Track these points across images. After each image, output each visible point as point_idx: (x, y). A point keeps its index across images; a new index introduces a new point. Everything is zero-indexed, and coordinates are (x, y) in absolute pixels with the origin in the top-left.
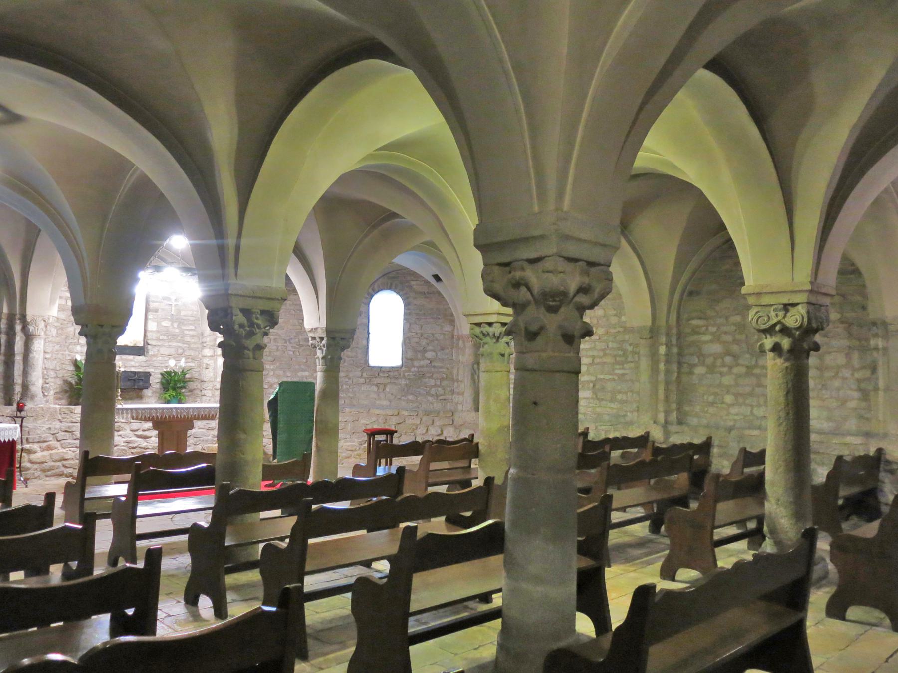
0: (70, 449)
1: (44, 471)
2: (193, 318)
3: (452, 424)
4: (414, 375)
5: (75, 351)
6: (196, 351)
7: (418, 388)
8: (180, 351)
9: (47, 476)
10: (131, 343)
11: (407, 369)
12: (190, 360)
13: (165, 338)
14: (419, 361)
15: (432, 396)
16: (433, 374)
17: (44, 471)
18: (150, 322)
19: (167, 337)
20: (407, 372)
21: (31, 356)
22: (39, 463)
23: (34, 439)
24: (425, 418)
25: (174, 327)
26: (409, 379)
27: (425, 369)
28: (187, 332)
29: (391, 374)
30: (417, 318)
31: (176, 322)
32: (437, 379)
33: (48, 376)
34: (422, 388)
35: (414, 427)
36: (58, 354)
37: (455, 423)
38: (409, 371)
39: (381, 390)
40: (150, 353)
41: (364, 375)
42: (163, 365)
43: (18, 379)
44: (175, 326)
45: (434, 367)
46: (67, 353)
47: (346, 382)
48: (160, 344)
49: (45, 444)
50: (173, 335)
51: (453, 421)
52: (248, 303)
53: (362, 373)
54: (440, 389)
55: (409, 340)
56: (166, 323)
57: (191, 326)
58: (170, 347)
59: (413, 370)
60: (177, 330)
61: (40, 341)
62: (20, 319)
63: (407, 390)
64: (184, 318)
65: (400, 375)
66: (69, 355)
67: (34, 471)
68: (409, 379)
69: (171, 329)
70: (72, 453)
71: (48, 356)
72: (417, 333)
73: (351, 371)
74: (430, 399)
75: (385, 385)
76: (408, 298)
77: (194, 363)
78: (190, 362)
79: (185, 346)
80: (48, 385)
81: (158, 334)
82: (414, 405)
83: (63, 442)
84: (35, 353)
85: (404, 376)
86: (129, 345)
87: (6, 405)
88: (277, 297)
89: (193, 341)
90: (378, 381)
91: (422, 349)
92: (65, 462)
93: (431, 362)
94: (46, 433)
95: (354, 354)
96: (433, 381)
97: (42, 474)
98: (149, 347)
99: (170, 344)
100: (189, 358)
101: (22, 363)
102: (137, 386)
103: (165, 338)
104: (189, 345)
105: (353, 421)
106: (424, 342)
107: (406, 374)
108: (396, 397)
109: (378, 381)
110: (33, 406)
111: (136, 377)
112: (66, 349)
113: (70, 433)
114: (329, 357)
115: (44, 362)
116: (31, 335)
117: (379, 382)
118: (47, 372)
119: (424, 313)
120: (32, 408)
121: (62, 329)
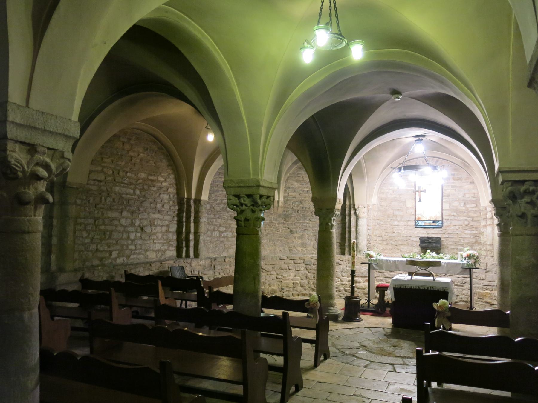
2: (475, 199)
5: (394, 225)
6: (478, 222)
8: (466, 223)
12: (474, 229)
13: (455, 214)
21: (358, 228)
22: (362, 289)
28: (470, 209)
31: (462, 202)
33: (370, 239)
36: (383, 226)
40: (445, 225)
42: (455, 233)
46: (389, 226)
48: (452, 218)
52: (237, 191)
56: (456, 204)
57: (473, 204)
58: (459, 220)
60: (464, 208)
61: (363, 219)
64: (469, 199)
66: (390, 227)
71: (369, 228)
78: (474, 230)
79: (469, 219)
80: (370, 245)
83: (377, 278)
84: (360, 226)
88: (253, 185)
89: (475, 215)
99: (459, 218)
100: (473, 228)
101: (355, 232)
102: (431, 246)
103: (455, 214)
104: (472, 218)
110: (360, 256)
111: (430, 240)
113: (382, 274)
114: (502, 224)
115: (367, 231)
120: (359, 257)
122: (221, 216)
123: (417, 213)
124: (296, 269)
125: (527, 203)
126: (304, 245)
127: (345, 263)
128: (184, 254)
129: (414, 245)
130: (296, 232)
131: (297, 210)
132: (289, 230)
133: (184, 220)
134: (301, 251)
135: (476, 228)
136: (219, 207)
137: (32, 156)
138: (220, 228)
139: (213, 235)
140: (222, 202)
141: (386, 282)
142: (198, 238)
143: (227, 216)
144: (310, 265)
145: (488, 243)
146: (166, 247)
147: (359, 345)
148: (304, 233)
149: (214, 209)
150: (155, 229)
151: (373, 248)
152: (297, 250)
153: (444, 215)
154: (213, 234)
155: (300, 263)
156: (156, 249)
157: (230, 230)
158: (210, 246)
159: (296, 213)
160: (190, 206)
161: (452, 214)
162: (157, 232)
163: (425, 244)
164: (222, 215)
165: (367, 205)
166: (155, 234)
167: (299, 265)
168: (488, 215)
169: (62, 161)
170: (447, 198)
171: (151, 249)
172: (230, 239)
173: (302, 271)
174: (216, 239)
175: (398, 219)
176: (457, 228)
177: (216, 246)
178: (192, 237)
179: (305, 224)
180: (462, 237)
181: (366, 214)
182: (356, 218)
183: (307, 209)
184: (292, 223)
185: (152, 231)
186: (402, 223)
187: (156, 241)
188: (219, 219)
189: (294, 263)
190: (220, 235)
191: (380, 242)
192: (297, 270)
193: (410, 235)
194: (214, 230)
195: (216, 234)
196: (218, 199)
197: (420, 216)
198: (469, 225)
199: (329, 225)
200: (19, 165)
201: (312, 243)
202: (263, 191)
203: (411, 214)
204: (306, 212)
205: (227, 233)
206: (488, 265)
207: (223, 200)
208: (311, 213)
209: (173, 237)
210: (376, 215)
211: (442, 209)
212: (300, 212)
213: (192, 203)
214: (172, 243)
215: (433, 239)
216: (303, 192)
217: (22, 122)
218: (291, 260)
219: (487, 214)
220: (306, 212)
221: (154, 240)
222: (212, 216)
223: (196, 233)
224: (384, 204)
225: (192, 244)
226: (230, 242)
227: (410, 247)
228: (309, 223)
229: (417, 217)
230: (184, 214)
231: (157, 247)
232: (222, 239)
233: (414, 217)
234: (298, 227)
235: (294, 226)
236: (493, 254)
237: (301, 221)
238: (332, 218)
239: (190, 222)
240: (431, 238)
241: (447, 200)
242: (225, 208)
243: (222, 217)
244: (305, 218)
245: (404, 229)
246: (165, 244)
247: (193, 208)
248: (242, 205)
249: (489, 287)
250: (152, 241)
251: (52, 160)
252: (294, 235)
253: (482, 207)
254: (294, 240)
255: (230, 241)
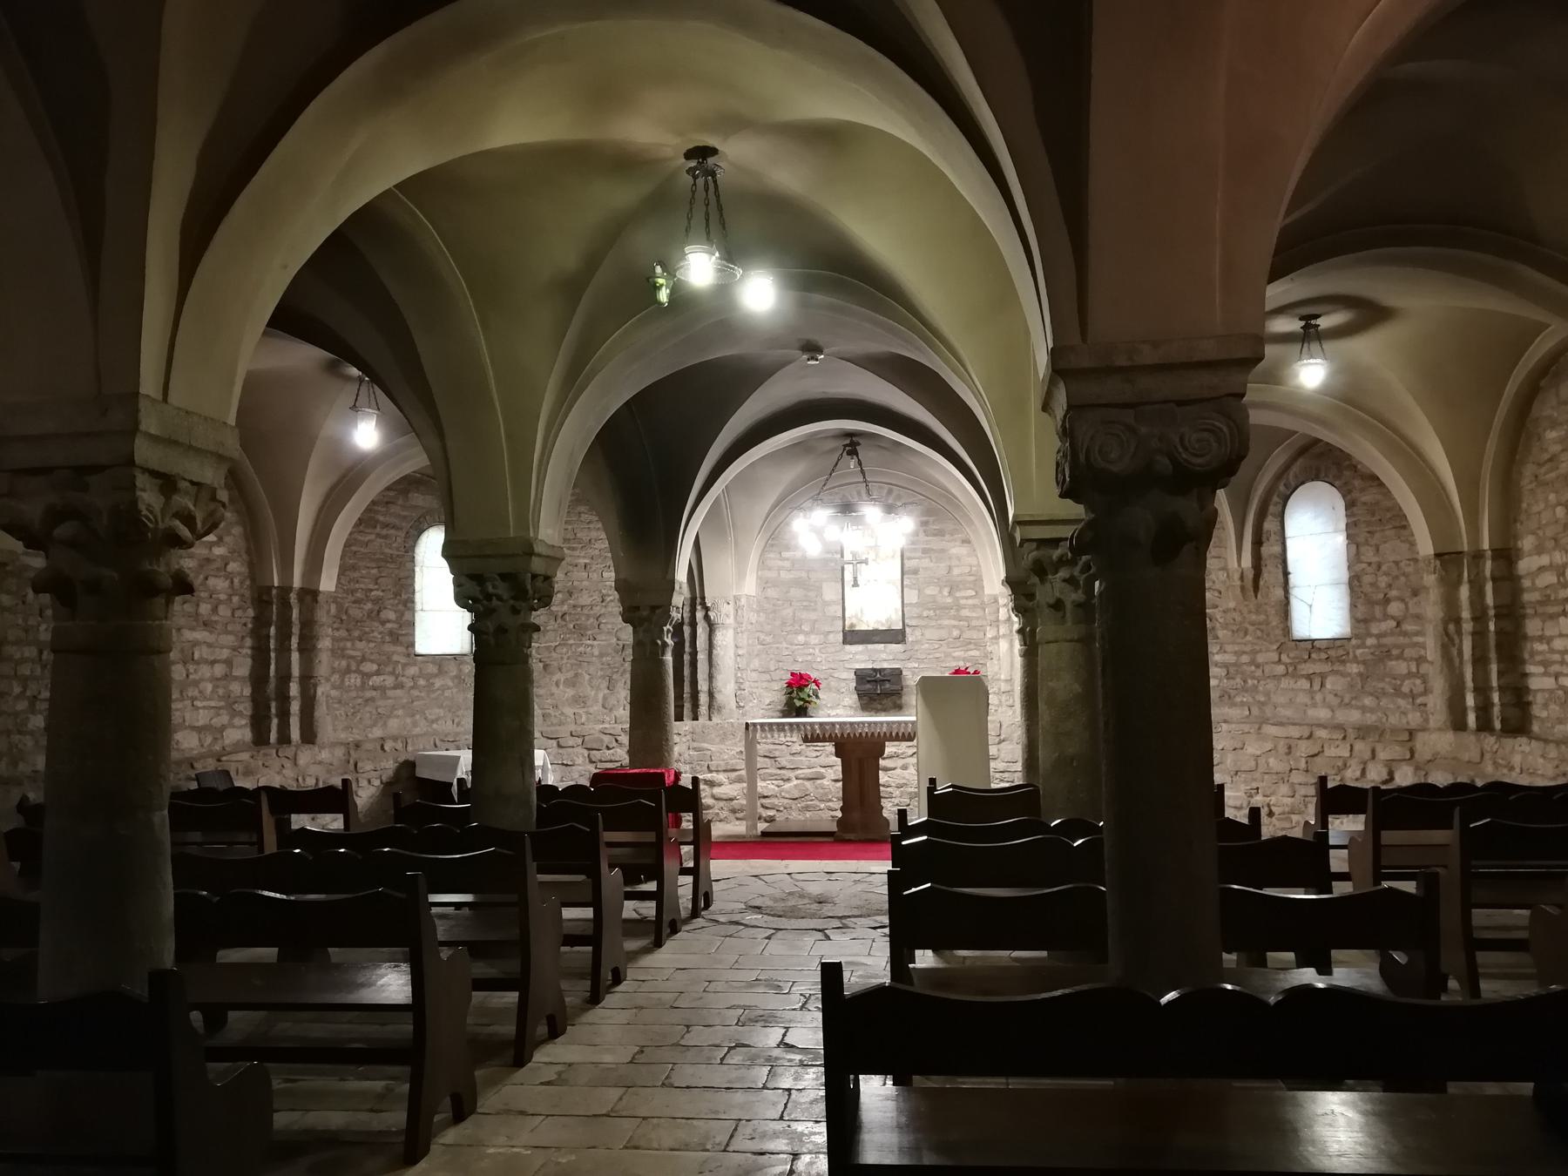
0: (773, 782)
1: (734, 811)
2: (972, 578)
3: (1409, 759)
4: (1372, 654)
5: (796, 642)
6: (979, 630)
7: (1382, 680)
8: (956, 633)
9: (737, 819)
10: (883, 625)
11: (1359, 642)
12: (972, 646)
13: (932, 613)
14: (1378, 624)
15: (1404, 696)
16: (1403, 650)
17: (734, 811)
18: (905, 589)
19: (934, 612)
20: (1358, 647)
21: (715, 652)
22: (726, 800)
23: (717, 767)
24: (1360, 746)
25: (943, 596)
26: (1364, 662)
27: (1388, 641)
28: (963, 602)
29: (1332, 653)
30: (1369, 532)
32: (1412, 659)
33: (743, 679)
34: (1387, 680)
35: (1340, 764)
37: (1416, 755)
38: (1363, 646)
39: (1317, 686)
40: (910, 639)
41: (1284, 657)
43: (703, 686)
44: (946, 593)
45: (1405, 634)
47: (1252, 672)
48: (922, 623)
49: (733, 775)
50: (942, 608)
51: (1412, 752)
53: (1280, 654)
54: (1418, 682)
55: (1359, 581)
58: (940, 627)
59: (1370, 641)
60: (949, 600)
61: (725, 631)
62: (700, 604)
63: (1362, 687)
64: (959, 579)
65: (1348, 653)
66: (787, 648)
67: (718, 811)
68: (1364, 662)
69: (939, 599)
70: (776, 788)
72: (1370, 564)
73: (1260, 651)
74: (1401, 702)
75: (1323, 676)
76: (1350, 492)
77: (979, 650)
78: (971, 650)
80: (743, 692)
81: (920, 609)
82: (1374, 718)
85: (1355, 656)
86: (881, 628)
87: (693, 720)
89: (974, 615)
90: (1309, 668)
91: (1381, 596)
92: (763, 801)
93: (1398, 624)
94: (735, 758)
95: (1262, 617)
96: (1405, 664)
97: (732, 817)
98: (907, 629)
99: (939, 622)
100: (970, 643)
101: (707, 664)
102: (881, 690)
103: (932, 613)
105: (1234, 750)
106: (1383, 581)
107: (1359, 652)
108: (1342, 701)
109: (1309, 668)
111: (878, 676)
112: (782, 639)
113: (773, 760)
114: (1028, 629)
115: (736, 660)
116: (713, 625)
117: (1311, 672)
118: (742, 674)
119: (1380, 520)
120: (718, 724)
121: (774, 612)
122: (366, 633)
123: (847, 615)
124: (565, 762)
125: (1065, 581)
126: (580, 700)
127: (684, 739)
128: (273, 736)
129: (843, 690)
130: (560, 669)
131: (560, 614)
132: (541, 665)
133: (272, 647)
134: (572, 716)
135: (975, 644)
136: (359, 608)
137: (168, 498)
138: (364, 664)
139: (347, 684)
140: (367, 596)
141: (782, 779)
142: (312, 691)
143: (380, 633)
144: (599, 750)
145: (1003, 677)
146: (224, 719)
147: (744, 907)
148: (580, 671)
149: (349, 616)
150: (196, 671)
151: (751, 701)
152: (562, 713)
153: (906, 616)
154: (346, 680)
155: (573, 747)
156: (200, 723)
157: (389, 669)
158: (337, 713)
159: (559, 620)
160: (290, 608)
161: (925, 614)
162: (202, 680)
163: (868, 686)
164: (367, 629)
165: (735, 597)
166: (196, 683)
167: (570, 750)
168: (1000, 615)
169: (212, 506)
170: (913, 576)
171: (187, 724)
172: (390, 693)
173: (579, 765)
174: (354, 694)
175: (806, 628)
176: (936, 647)
177: (354, 713)
178: (294, 689)
179: (581, 649)
180: (947, 665)
181: (732, 617)
182: (708, 629)
183: (586, 611)
184: (547, 648)
185: (187, 676)
186: (814, 639)
187: (198, 703)
188: (361, 641)
189: (559, 746)
190: (363, 683)
191: (765, 684)
192: (567, 765)
193: (833, 667)
194: (348, 671)
195: (354, 680)
196: (356, 590)
197: (854, 621)
198: (961, 639)
199: (658, 644)
200: (151, 517)
201: (601, 696)
202: (537, 565)
203: (835, 617)
204: (583, 619)
205: (382, 678)
206: (1004, 727)
207: (372, 590)
208: (597, 620)
209: (241, 690)
210: (754, 622)
211: (903, 602)
212: (567, 618)
213: (293, 597)
214: (239, 707)
215: (885, 672)
216: (575, 569)
217: (158, 433)
218: (552, 739)
219: (998, 612)
220: (583, 619)
221: (193, 699)
222: (343, 633)
223: (308, 680)
224: (771, 593)
225: (295, 707)
226: (390, 701)
227: (835, 695)
228: (592, 646)
229: (847, 623)
230: (273, 630)
231: (202, 718)
232: (369, 694)
233: (840, 623)
234: (565, 657)
235: (554, 654)
236: (1014, 701)
237: (571, 642)
238: (665, 628)
239: (289, 650)
240: (880, 671)
241: (914, 582)
242: (375, 613)
243: (366, 635)
244: (582, 632)
245: (820, 651)
246: (221, 711)
247: (295, 613)
248: (489, 597)
249: (1006, 775)
250: (188, 703)
251: (195, 506)
252: (555, 679)
253: (988, 595)
254: (554, 689)
255: (389, 698)
